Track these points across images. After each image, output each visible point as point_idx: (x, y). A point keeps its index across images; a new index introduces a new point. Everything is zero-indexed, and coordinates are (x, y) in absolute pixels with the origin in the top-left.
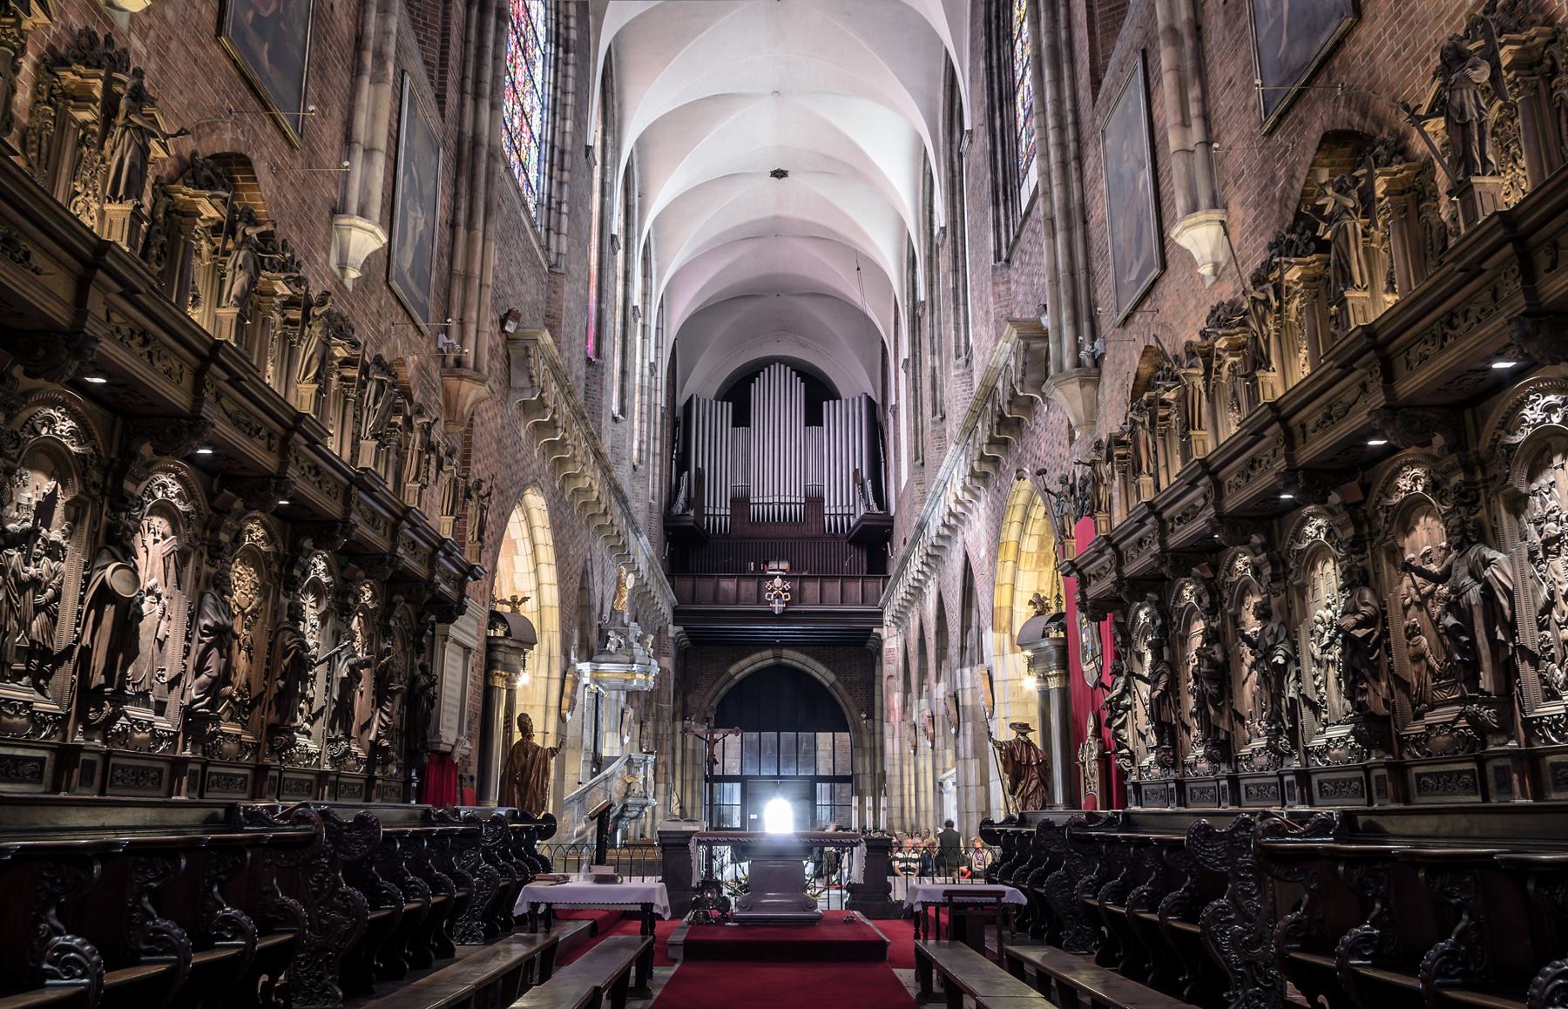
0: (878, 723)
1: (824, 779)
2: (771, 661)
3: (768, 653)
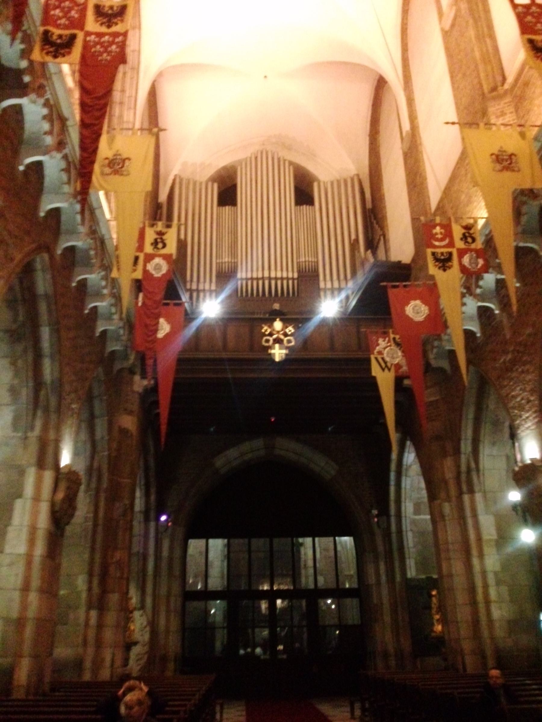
0: (393, 520)
2: (262, 453)
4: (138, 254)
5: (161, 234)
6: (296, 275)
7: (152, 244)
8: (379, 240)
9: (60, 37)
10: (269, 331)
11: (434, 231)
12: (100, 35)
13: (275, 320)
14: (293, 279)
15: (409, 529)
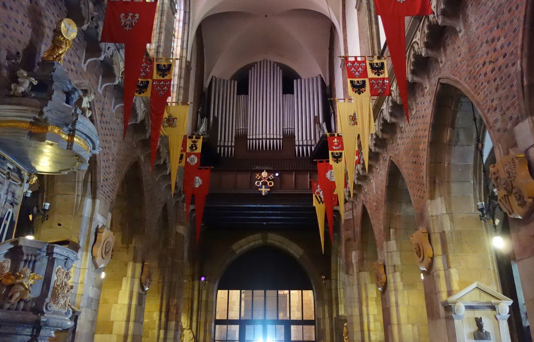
0: (333, 282)
1: (296, 322)
2: (261, 241)
3: (258, 236)
4: (183, 153)
5: (195, 142)
6: (282, 137)
7: (190, 148)
8: (332, 114)
9: (142, 82)
10: (259, 177)
11: (334, 141)
12: (159, 81)
13: (263, 171)
14: (280, 139)
15: (341, 287)
